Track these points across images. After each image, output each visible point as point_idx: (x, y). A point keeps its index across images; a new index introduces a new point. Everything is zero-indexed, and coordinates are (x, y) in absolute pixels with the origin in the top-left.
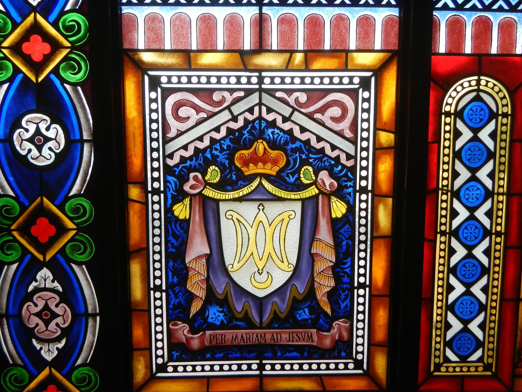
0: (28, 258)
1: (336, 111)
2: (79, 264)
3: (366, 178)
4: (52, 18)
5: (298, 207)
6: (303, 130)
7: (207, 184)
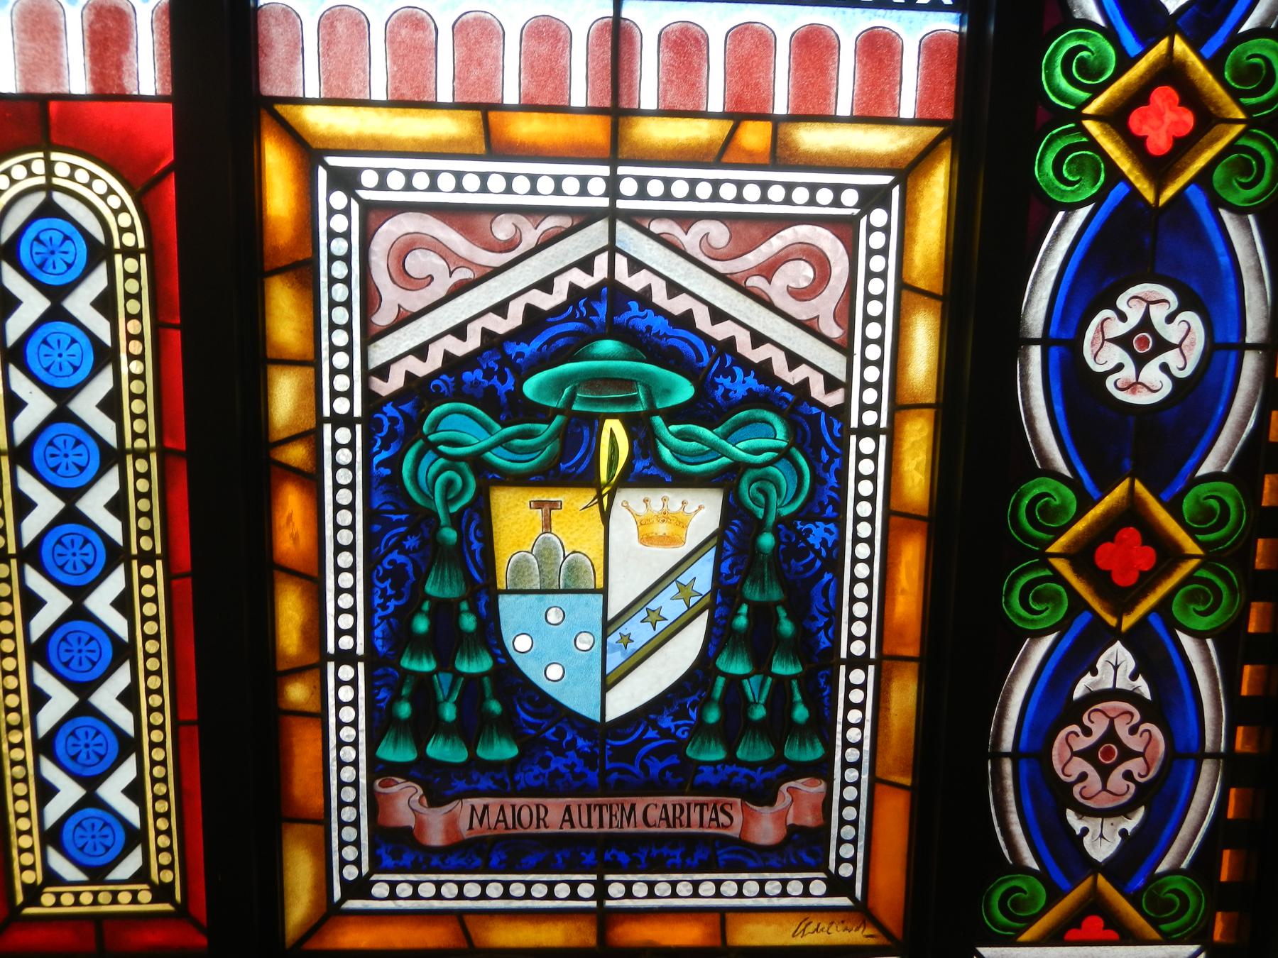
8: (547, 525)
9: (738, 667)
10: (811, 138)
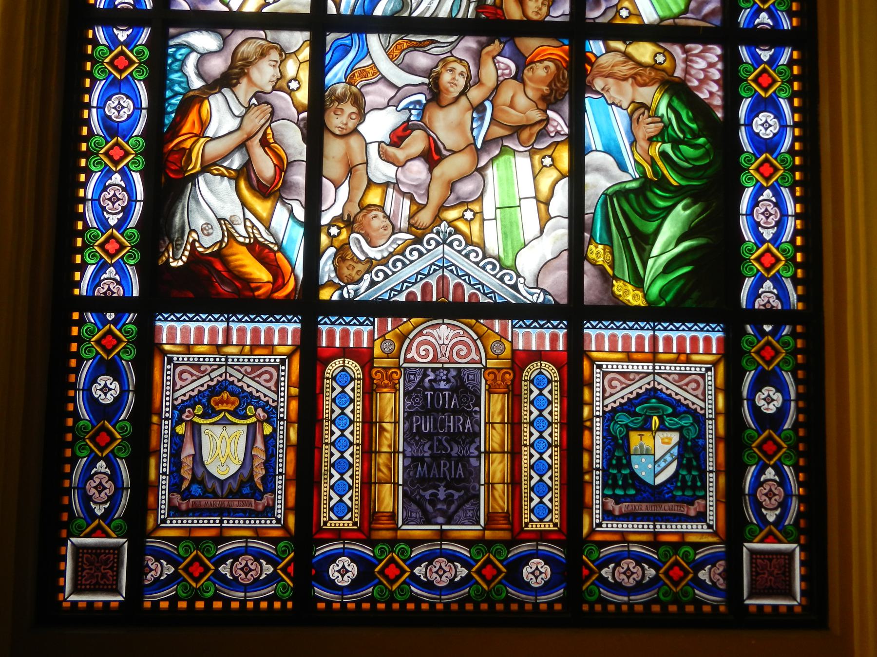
0: (93, 455)
1: (267, 376)
2: (121, 459)
3: (283, 413)
4: (119, 327)
5: (245, 428)
6: (249, 386)
7: (195, 415)
8: (641, 440)
9: (684, 473)
10: (695, 357)
